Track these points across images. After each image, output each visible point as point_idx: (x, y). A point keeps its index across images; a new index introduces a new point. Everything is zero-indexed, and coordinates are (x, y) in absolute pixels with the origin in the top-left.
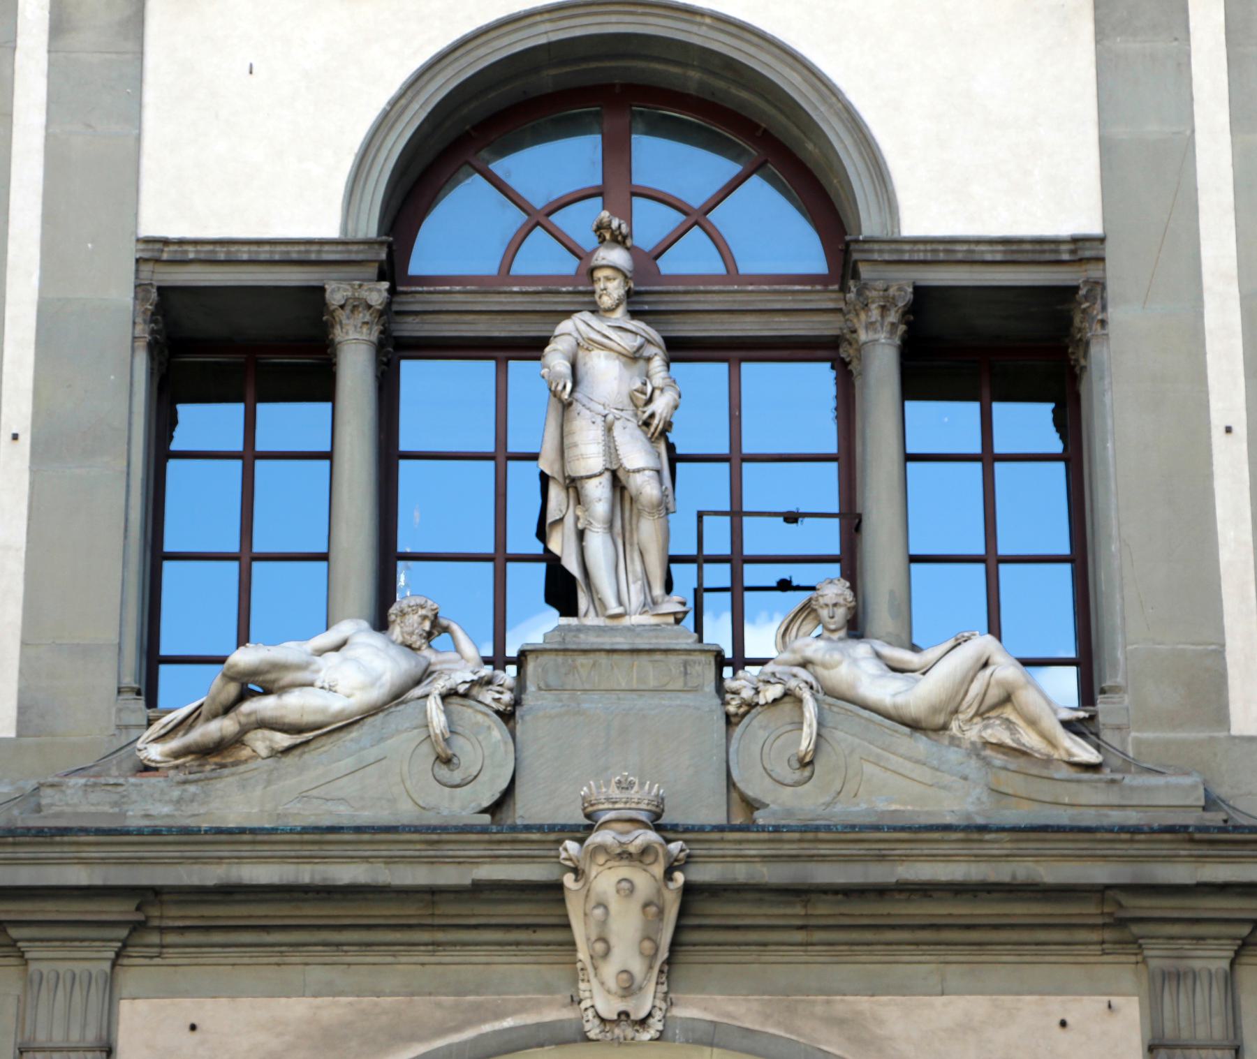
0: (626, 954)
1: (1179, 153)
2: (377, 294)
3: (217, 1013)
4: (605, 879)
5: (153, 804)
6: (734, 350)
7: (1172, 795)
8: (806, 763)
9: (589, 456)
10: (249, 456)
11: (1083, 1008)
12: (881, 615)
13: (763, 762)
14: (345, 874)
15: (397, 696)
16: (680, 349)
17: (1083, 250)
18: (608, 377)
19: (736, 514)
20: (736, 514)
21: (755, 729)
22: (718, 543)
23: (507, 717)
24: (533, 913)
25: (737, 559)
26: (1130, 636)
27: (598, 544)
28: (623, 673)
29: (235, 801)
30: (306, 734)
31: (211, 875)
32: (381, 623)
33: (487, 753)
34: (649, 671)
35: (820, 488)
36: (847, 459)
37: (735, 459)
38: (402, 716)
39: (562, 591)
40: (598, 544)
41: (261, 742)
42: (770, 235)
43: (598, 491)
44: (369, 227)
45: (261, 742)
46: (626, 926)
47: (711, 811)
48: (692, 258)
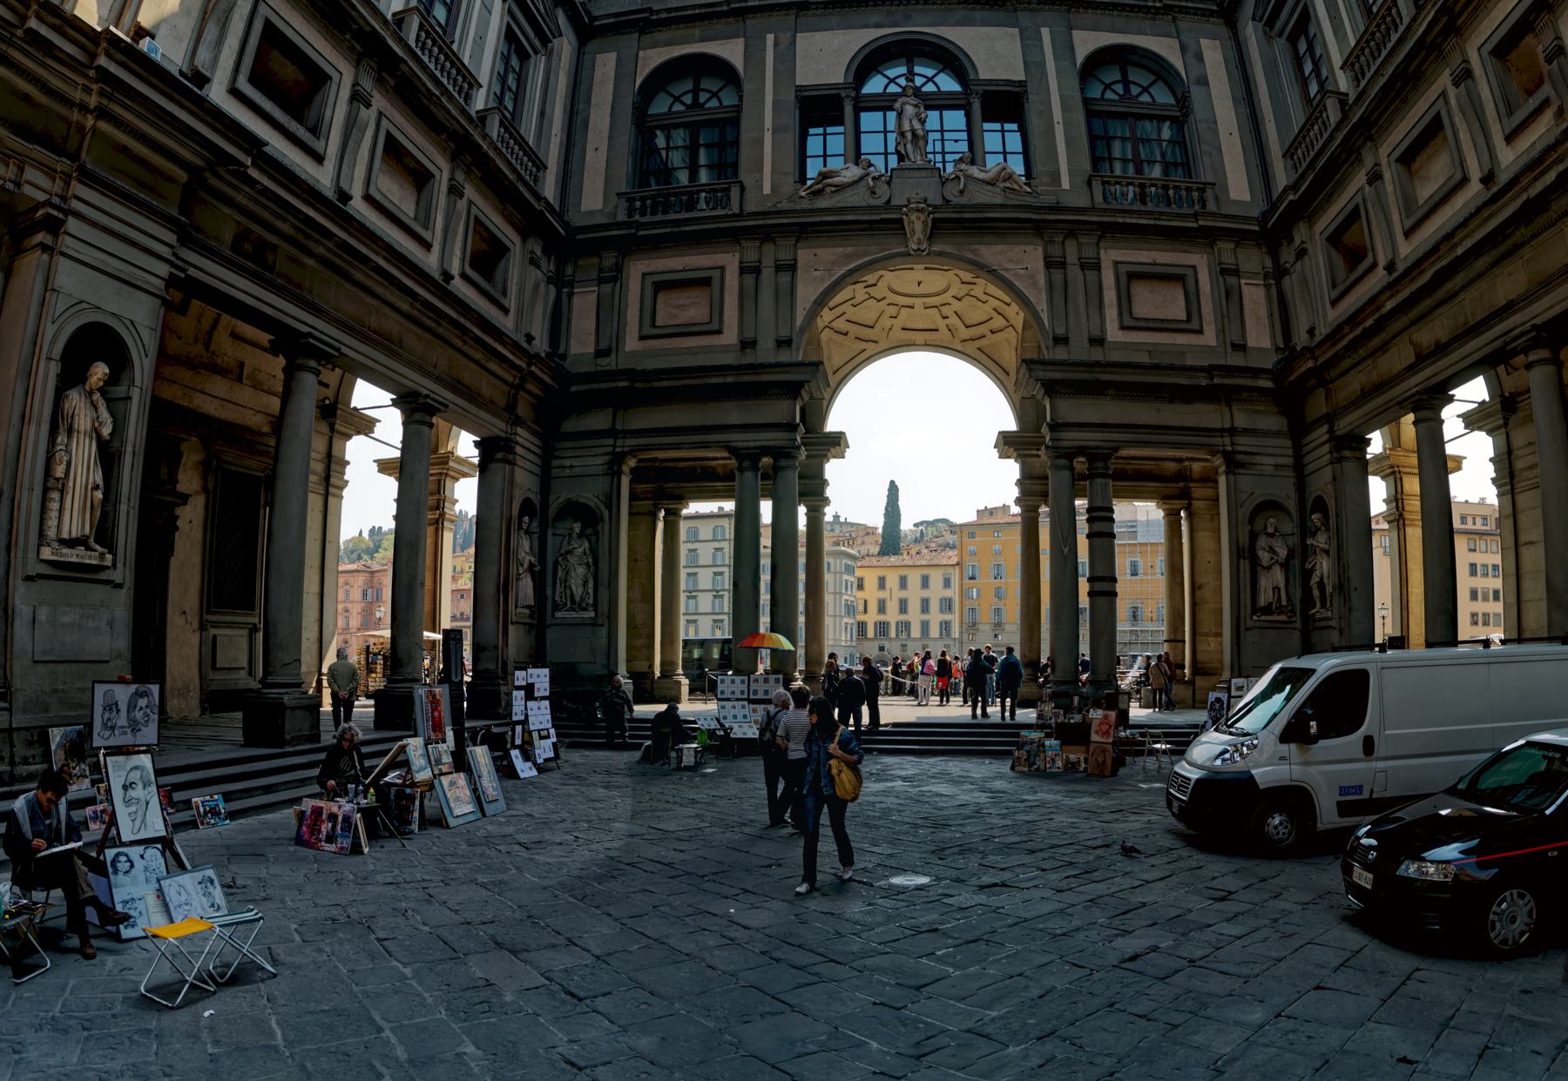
0: (919, 234)
1: (1042, 65)
2: (853, 94)
3: (820, 251)
4: (913, 217)
6: (941, 108)
7: (1049, 200)
8: (962, 192)
9: (906, 127)
10: (825, 135)
11: (1029, 248)
12: (979, 161)
13: (951, 192)
14: (849, 218)
15: (861, 179)
16: (928, 108)
17: (1021, 84)
18: (910, 110)
19: (943, 140)
20: (943, 140)
21: (949, 186)
22: (938, 149)
23: (889, 183)
24: (896, 226)
25: (943, 153)
26: (1038, 167)
27: (909, 146)
28: (916, 174)
29: (823, 203)
30: (841, 188)
31: (818, 219)
32: (857, 164)
33: (883, 191)
34: (923, 173)
35: (964, 136)
36: (969, 130)
37: (942, 131)
38: (863, 183)
39: (901, 158)
40: (909, 146)
41: (828, 190)
42: (948, 84)
43: (909, 136)
44: (851, 80)
45: (828, 190)
46: (918, 227)
47: (939, 202)
48: (930, 88)
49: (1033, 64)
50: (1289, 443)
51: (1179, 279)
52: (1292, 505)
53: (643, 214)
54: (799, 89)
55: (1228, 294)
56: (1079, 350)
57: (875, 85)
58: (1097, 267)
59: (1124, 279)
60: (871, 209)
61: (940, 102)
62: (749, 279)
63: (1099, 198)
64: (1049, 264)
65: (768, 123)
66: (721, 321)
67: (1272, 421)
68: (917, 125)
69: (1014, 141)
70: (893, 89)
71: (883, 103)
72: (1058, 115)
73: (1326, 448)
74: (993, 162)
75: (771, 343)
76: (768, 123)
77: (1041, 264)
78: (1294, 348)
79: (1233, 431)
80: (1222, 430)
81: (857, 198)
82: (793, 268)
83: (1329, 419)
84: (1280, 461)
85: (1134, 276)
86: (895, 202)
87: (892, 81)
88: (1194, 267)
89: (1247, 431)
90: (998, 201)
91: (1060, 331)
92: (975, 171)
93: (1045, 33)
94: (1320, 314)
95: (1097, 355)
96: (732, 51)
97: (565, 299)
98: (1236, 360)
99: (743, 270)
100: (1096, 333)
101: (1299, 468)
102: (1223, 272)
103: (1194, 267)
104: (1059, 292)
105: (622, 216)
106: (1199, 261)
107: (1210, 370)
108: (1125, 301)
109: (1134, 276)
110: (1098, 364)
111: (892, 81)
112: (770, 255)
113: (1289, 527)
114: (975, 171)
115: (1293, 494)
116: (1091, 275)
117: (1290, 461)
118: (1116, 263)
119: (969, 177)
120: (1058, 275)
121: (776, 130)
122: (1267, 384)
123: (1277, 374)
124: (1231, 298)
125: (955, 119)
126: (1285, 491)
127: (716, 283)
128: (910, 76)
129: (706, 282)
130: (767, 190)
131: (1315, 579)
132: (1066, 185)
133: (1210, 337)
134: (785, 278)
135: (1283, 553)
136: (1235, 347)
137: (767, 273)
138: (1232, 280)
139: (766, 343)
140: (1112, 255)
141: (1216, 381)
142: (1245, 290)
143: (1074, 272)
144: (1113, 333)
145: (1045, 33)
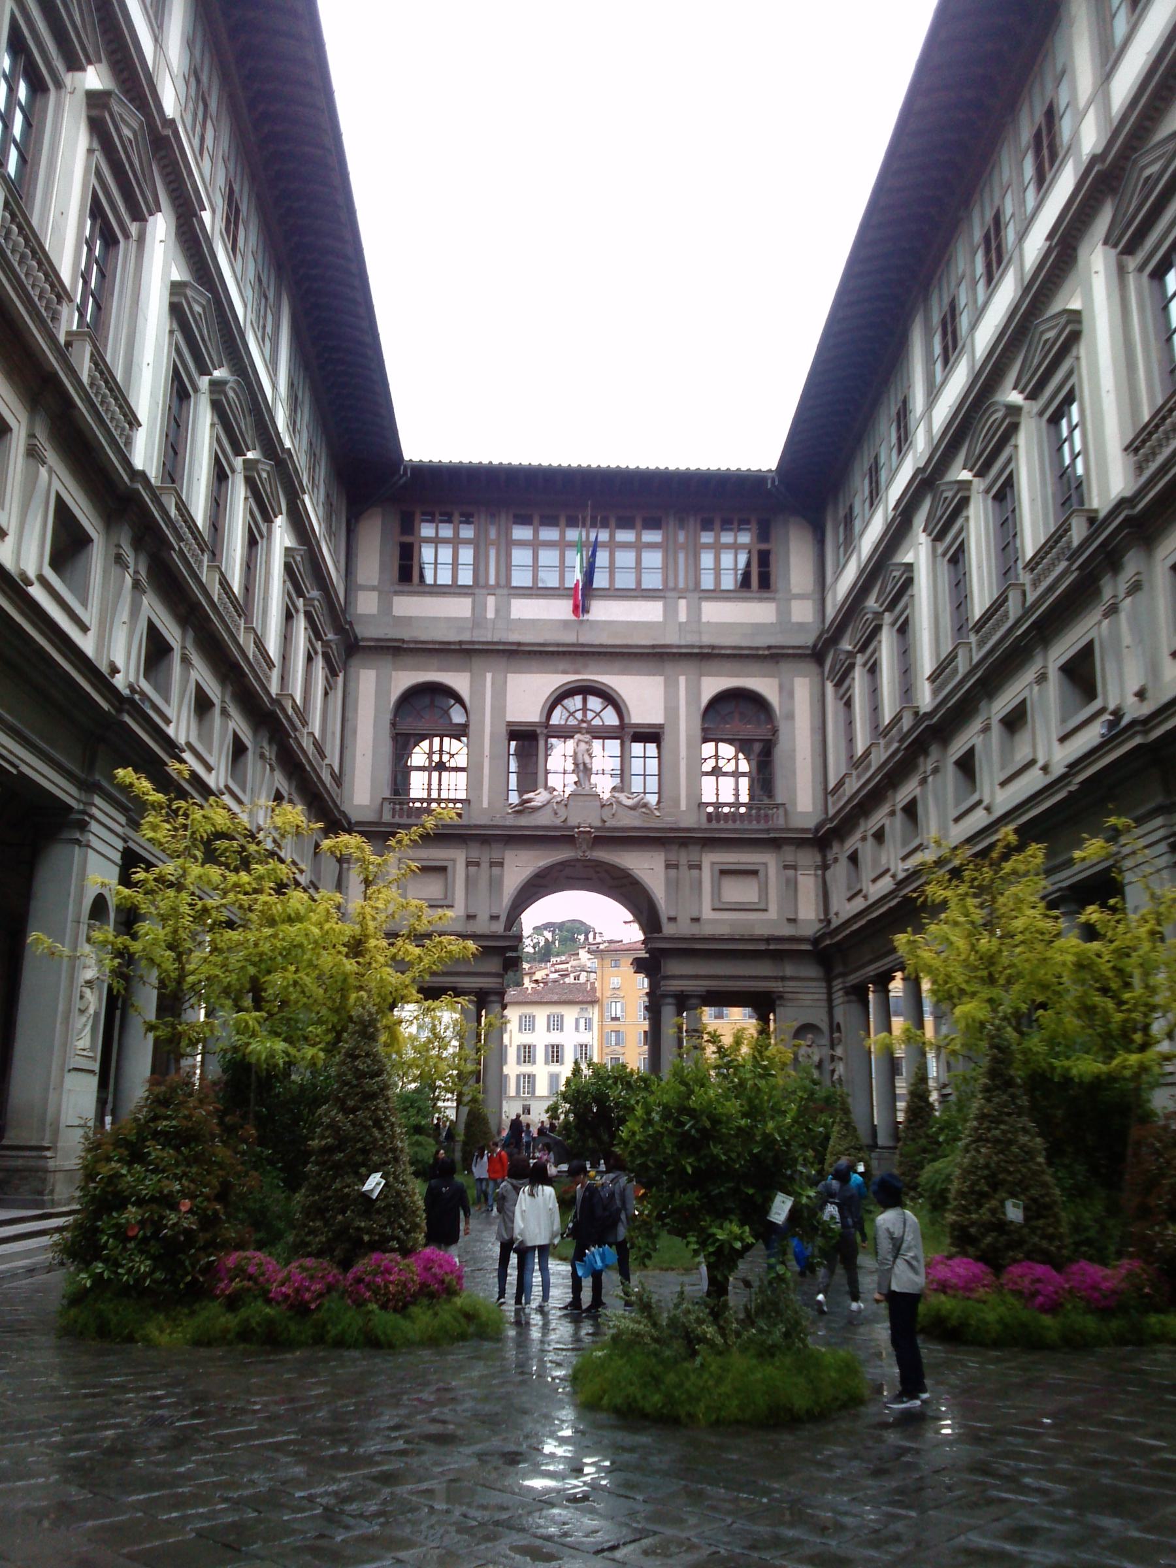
5: (510, 821)
11: (655, 854)
47: (598, 824)
49: (671, 709)
50: (824, 984)
51: (754, 873)
52: (824, 1026)
53: (401, 817)
54: (509, 724)
55: (788, 881)
56: (684, 928)
57: (557, 718)
58: (699, 867)
59: (717, 873)
60: (555, 828)
61: (603, 734)
62: (472, 869)
63: (704, 819)
64: (668, 866)
65: (487, 751)
66: (453, 899)
67: (812, 971)
68: (587, 760)
69: (653, 766)
70: (572, 722)
71: (565, 733)
72: (683, 752)
73: (840, 993)
74: (637, 785)
75: (486, 917)
76: (487, 751)
77: (663, 865)
78: (829, 922)
79: (783, 979)
80: (776, 978)
81: (543, 819)
82: (501, 864)
83: (844, 975)
84: (816, 996)
85: (723, 872)
86: (572, 822)
87: (572, 714)
88: (765, 864)
89: (792, 979)
90: (637, 823)
91: (672, 914)
92: (622, 797)
93: (682, 680)
94: (844, 909)
95: (695, 930)
96: (459, 681)
97: (344, 874)
98: (787, 931)
99: (468, 864)
100: (695, 915)
101: (830, 1000)
102: (786, 867)
103: (765, 864)
104: (673, 886)
105: (387, 817)
106: (768, 861)
107: (768, 940)
108: (717, 891)
109: (723, 872)
110: (693, 939)
111: (572, 714)
112: (484, 855)
113: (825, 1041)
114: (622, 797)
115: (825, 1018)
116: (695, 872)
117: (824, 997)
118: (713, 863)
119: (619, 803)
120: (673, 872)
121: (492, 758)
122: (808, 947)
123: (816, 941)
124: (792, 886)
125: (614, 746)
126: (819, 1017)
127: (450, 870)
128: (585, 709)
129: (443, 869)
130: (485, 805)
131: (836, 1077)
132: (683, 807)
133: (773, 914)
134: (496, 870)
135: (816, 1058)
136: (790, 920)
137: (485, 866)
138: (791, 872)
139: (483, 916)
140: (711, 860)
141: (772, 947)
142: (801, 879)
143: (684, 869)
144: (707, 913)
145: (682, 680)
